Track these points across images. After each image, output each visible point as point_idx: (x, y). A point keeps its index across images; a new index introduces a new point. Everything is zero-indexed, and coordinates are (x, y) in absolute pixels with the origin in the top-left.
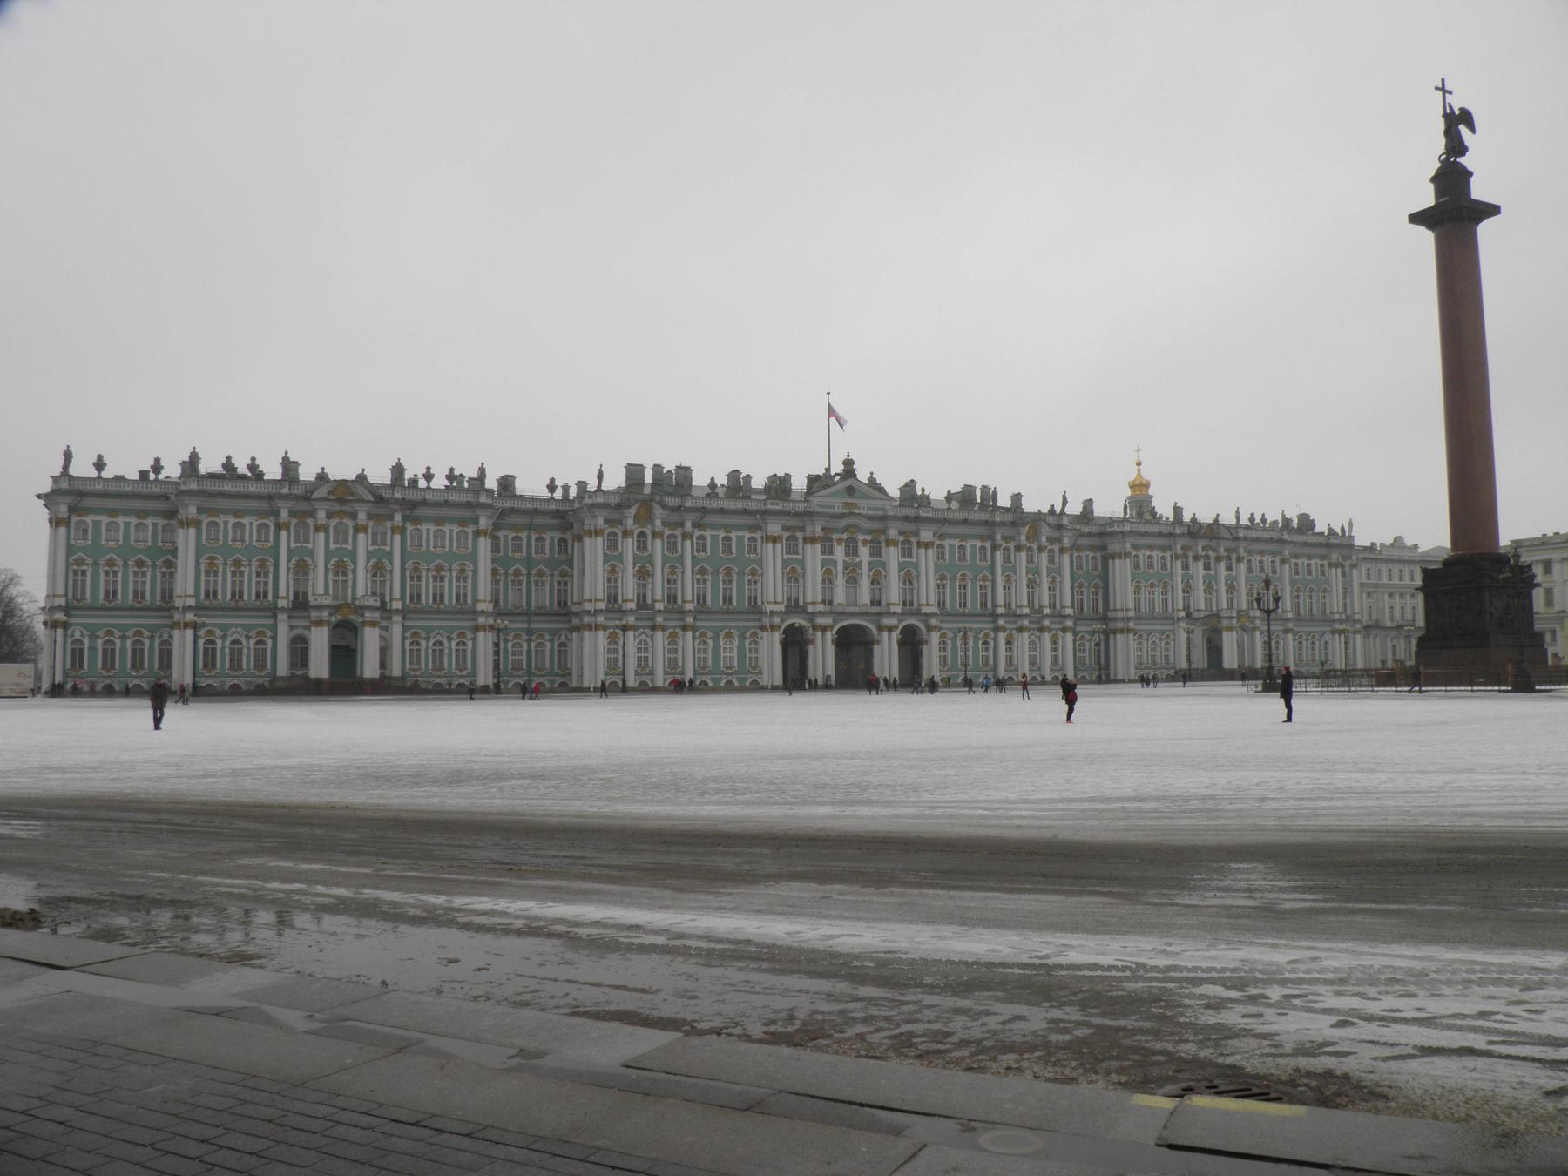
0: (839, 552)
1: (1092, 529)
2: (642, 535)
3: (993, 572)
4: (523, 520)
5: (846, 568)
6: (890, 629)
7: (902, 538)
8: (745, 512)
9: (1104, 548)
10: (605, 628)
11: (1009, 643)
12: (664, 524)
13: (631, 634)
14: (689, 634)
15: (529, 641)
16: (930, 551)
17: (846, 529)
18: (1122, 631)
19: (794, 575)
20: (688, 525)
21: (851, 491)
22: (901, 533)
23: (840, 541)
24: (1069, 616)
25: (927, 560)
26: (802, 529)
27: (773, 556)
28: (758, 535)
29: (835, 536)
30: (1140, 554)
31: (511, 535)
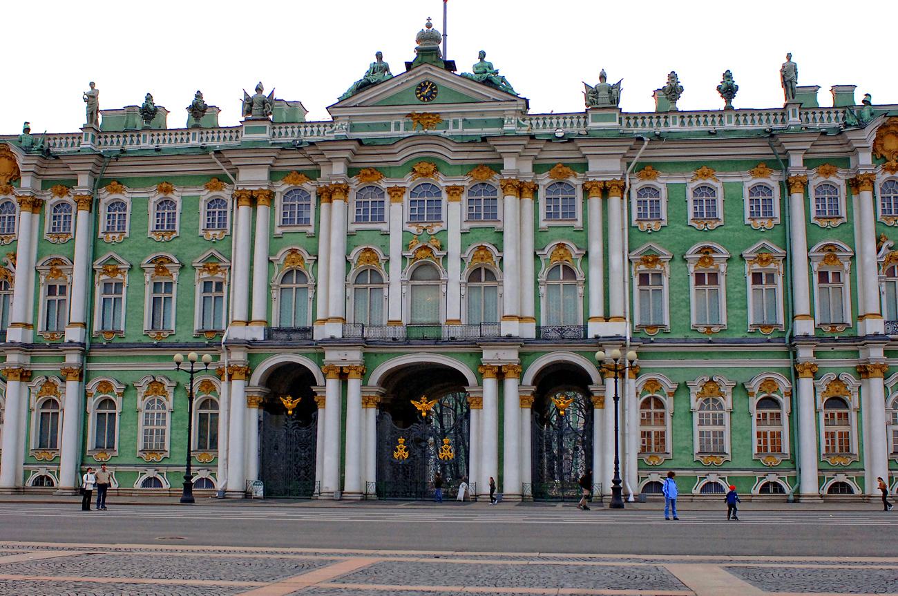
0: (397, 214)
3: (786, 242)
5: (407, 247)
7: (545, 180)
11: (837, 402)
14: (72, 386)
17: (411, 167)
19: (295, 273)
21: (427, 91)
22: (537, 168)
23: (396, 192)
25: (608, 228)
26: (314, 174)
27: (250, 235)
28: (226, 193)
29: (384, 184)
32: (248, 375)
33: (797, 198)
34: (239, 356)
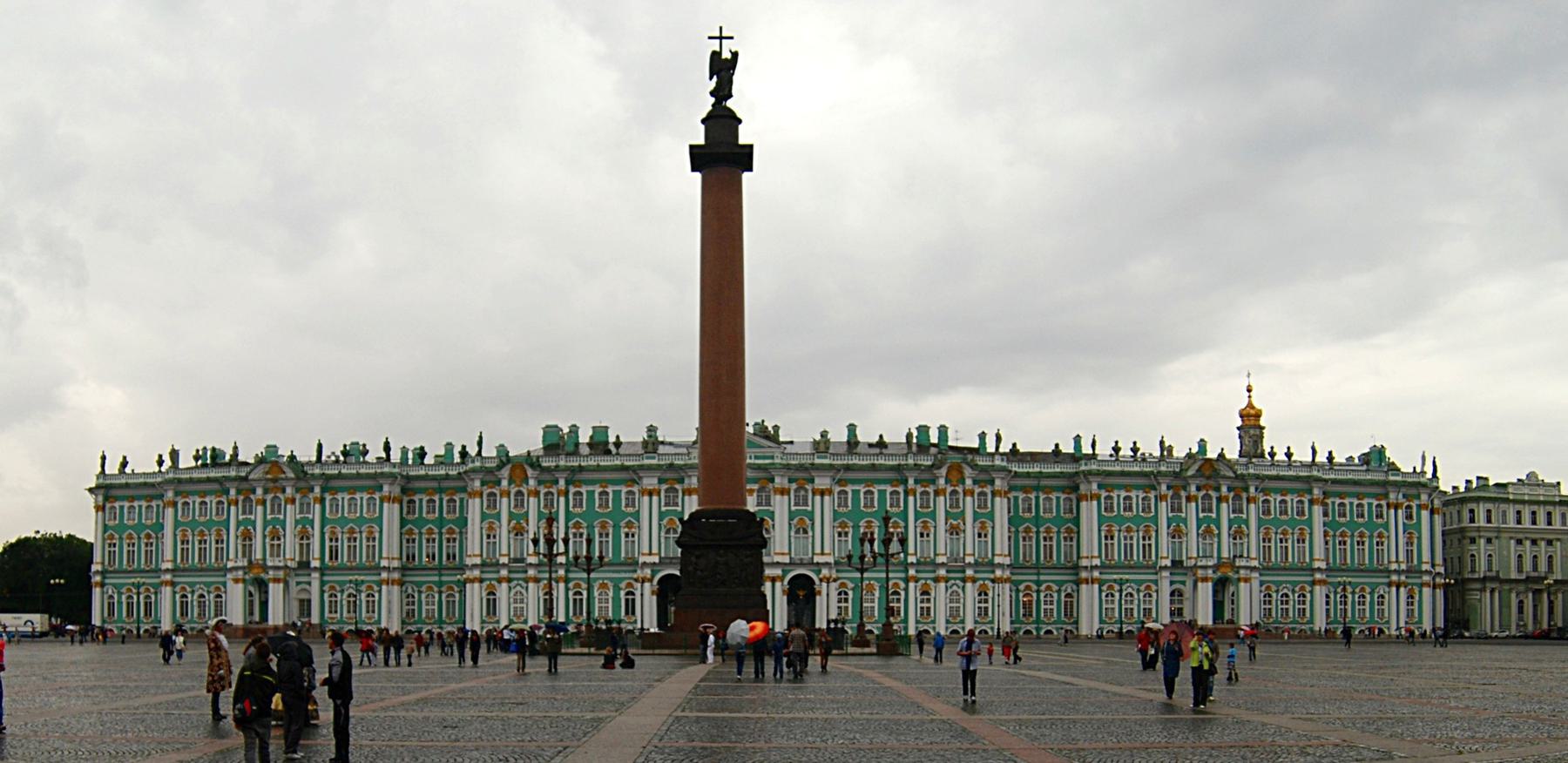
1: (1069, 469)
2: (519, 493)
3: (906, 521)
4: (435, 484)
6: (773, 580)
7: (794, 486)
8: (624, 468)
9: (1076, 488)
10: (481, 581)
12: (540, 483)
13: (504, 585)
14: (562, 585)
15: (440, 593)
16: (827, 498)
18: (1087, 581)
20: (562, 482)
22: (790, 481)
24: (1000, 566)
26: (681, 481)
28: (635, 489)
30: (1114, 495)
31: (426, 498)
32: (651, 580)
33: (911, 499)
34: (648, 572)
